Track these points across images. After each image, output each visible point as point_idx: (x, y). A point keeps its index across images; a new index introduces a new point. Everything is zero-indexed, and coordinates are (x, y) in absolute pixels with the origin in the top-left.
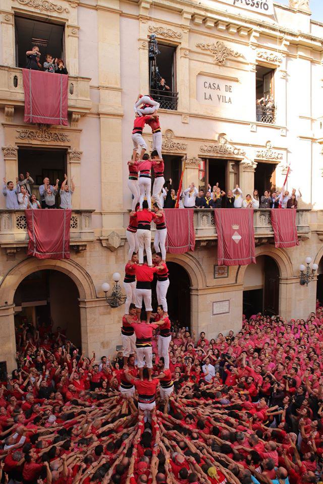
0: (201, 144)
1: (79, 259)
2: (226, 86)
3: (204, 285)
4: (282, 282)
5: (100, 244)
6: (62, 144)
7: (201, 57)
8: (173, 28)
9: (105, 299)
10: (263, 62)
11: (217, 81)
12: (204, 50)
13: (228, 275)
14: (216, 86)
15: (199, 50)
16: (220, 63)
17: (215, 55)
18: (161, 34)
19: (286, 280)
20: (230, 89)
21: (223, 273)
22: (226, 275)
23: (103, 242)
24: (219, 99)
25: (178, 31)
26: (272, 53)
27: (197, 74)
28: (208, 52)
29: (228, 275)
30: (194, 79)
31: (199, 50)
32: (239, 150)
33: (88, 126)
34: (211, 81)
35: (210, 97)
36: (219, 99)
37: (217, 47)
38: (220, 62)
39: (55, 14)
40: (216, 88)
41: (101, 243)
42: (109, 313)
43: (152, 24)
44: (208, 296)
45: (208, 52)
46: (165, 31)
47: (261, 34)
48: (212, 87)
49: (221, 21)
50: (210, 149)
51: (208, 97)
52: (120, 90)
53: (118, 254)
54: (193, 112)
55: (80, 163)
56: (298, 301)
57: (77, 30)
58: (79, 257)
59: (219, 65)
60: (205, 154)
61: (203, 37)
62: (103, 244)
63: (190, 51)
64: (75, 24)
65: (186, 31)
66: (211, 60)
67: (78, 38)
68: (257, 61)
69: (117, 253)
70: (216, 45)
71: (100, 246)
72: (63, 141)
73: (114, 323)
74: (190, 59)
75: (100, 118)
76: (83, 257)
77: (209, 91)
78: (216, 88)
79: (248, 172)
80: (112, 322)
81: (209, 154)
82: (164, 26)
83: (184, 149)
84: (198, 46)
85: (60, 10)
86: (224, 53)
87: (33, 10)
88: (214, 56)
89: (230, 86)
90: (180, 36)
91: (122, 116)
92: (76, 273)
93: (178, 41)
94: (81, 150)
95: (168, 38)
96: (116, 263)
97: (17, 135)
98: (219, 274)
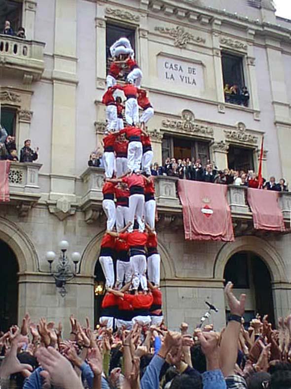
0: (165, 119)
1: (21, 223)
2: (189, 68)
3: (173, 274)
4: (276, 286)
5: (47, 210)
6: (12, 103)
7: (160, 39)
8: (132, 13)
9: (50, 274)
10: (228, 48)
11: (179, 64)
12: (163, 33)
15: (158, 32)
16: (180, 46)
17: (176, 38)
19: (279, 284)
20: (194, 72)
23: (50, 206)
24: (182, 80)
26: (236, 41)
27: (157, 54)
28: (168, 35)
31: (158, 32)
32: (207, 128)
33: (42, 90)
34: (174, 62)
36: (182, 80)
37: (177, 30)
38: (181, 45)
40: (178, 69)
41: (48, 209)
45: (168, 35)
46: (123, 13)
47: (223, 22)
49: (179, 8)
50: (173, 124)
52: (76, 60)
53: (68, 224)
55: (30, 123)
57: (34, 5)
58: (23, 221)
59: (181, 48)
60: (168, 129)
62: (50, 209)
63: (148, 33)
65: (144, 15)
66: (171, 43)
69: (66, 223)
70: (176, 30)
71: (47, 213)
72: (14, 100)
73: (59, 306)
74: (148, 40)
75: (53, 84)
76: (26, 222)
77: (170, 72)
78: (178, 69)
80: (57, 305)
81: (172, 130)
82: (121, 9)
84: (157, 29)
86: (185, 37)
88: (174, 40)
89: (193, 69)
91: (77, 83)
94: (31, 110)
95: (125, 20)
96: (65, 233)
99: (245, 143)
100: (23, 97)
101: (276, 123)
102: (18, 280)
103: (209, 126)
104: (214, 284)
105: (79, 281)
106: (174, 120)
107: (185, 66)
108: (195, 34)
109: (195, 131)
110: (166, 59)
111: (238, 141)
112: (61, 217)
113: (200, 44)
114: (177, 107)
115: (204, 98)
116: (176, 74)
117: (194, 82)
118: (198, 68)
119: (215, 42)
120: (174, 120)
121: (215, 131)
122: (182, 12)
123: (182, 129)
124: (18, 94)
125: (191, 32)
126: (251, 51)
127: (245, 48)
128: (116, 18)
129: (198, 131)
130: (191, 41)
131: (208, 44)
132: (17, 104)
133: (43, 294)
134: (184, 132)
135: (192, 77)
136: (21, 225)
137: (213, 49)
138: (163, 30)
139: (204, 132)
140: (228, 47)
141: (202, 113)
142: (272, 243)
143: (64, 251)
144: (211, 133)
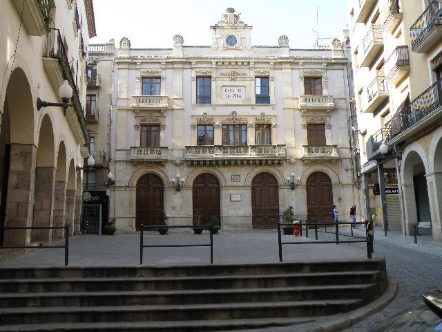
8: (207, 70)
26: (263, 69)
33: (168, 115)
34: (229, 88)
77: (228, 93)
90: (211, 72)
92: (162, 175)
107: (236, 89)
110: (225, 88)
113: (244, 76)
114: (228, 111)
116: (231, 94)
119: (252, 74)
126: (272, 73)
131: (248, 75)
136: (163, 169)
141: (241, 112)
142: (277, 168)
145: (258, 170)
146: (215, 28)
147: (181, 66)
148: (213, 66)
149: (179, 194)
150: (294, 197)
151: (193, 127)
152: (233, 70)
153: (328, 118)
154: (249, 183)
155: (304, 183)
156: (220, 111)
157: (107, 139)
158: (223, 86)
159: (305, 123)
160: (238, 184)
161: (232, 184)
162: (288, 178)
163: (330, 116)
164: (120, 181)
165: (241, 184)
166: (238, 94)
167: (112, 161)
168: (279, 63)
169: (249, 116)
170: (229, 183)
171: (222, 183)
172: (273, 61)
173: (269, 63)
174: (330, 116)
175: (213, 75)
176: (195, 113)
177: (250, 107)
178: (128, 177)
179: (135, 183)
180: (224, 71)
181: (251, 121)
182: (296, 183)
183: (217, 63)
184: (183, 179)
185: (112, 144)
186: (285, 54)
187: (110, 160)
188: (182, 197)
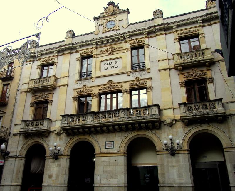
0: (100, 88)
6: (47, 99)
7: (102, 55)
8: (89, 50)
11: (110, 61)
13: (114, 147)
14: (110, 63)
15: (101, 53)
16: (110, 54)
18: (84, 54)
21: (110, 146)
22: (113, 147)
25: (92, 50)
28: (106, 52)
29: (114, 147)
30: (98, 64)
31: (101, 53)
34: (108, 62)
35: (107, 68)
39: (51, 61)
42: (54, 162)
43: (81, 52)
44: (102, 158)
45: (106, 52)
48: (108, 64)
51: (106, 68)
54: (97, 75)
56: (171, 167)
57: (56, 63)
59: (111, 55)
61: (103, 48)
63: (97, 55)
64: (56, 61)
67: (57, 65)
68: (130, 46)
72: (47, 98)
77: (106, 67)
79: (125, 94)
81: (103, 91)
82: (85, 51)
83: (91, 91)
85: (52, 59)
87: (45, 62)
90: (92, 51)
92: (45, 145)
93: (92, 53)
97: (35, 98)
98: (108, 146)
99: (140, 86)
100: (50, 96)
101: (159, 70)
102: (46, 158)
103: (121, 84)
104: (119, 155)
105: (62, 157)
106: (103, 86)
107: (113, 61)
108: (118, 46)
109: (113, 88)
111: (136, 86)
112: (59, 134)
113: (120, 49)
114: (105, 81)
115: (120, 72)
116: (109, 66)
117: (117, 67)
118: (119, 60)
119: (127, 45)
120: (103, 86)
121: (123, 85)
122: (111, 40)
123: (107, 89)
124: (48, 95)
125: (115, 46)
127: (144, 41)
128: (84, 54)
129: (115, 87)
130: (116, 50)
131: (124, 48)
132: (48, 98)
133: (51, 163)
134: (108, 90)
135: (116, 65)
137: (126, 49)
138: (103, 51)
139: (118, 87)
140: (134, 45)
143: (55, 147)
144: (122, 86)
145: (132, 135)
146: (96, 19)
147: (69, 51)
148: (94, 46)
149: (56, 163)
150: (174, 164)
151: (74, 98)
152: (111, 46)
153: (208, 72)
154: (123, 149)
155: (186, 147)
156: (98, 82)
157: (10, 117)
158: (101, 61)
159: (183, 80)
160: (112, 151)
161: (105, 151)
162: (165, 142)
163: (211, 70)
164: (13, 152)
165: (116, 150)
166: (116, 65)
167: (11, 135)
168: (152, 32)
169: (123, 82)
170: (104, 151)
171: (97, 151)
172: (146, 31)
173: (142, 34)
174: (211, 70)
175: (94, 53)
176: (76, 87)
177: (126, 75)
178: (19, 148)
179: (24, 153)
180: (104, 49)
181: (126, 86)
182: (176, 147)
183: (97, 44)
184: (59, 148)
185: (13, 121)
186: (159, 21)
187: (10, 133)
188: (59, 166)
